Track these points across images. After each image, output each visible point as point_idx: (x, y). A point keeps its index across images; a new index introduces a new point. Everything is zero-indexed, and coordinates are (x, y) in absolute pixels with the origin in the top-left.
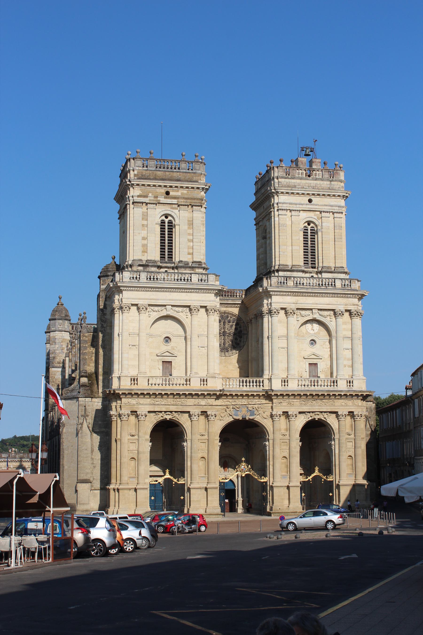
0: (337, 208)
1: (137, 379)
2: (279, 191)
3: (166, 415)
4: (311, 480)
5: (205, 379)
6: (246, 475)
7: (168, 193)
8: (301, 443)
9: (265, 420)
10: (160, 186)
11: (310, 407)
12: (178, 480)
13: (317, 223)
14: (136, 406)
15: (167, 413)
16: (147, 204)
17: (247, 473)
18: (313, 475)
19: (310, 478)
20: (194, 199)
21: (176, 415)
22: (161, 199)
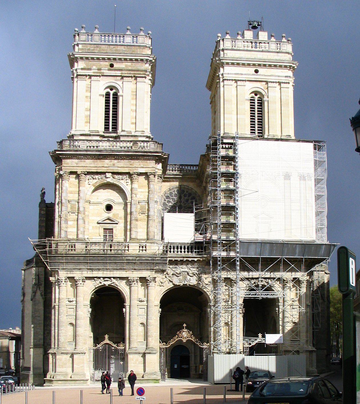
0: (284, 78)
2: (224, 61)
3: (105, 281)
7: (112, 66)
10: (104, 59)
12: (118, 346)
13: (264, 93)
15: (106, 279)
16: (90, 76)
17: (188, 339)
20: (138, 71)
21: (114, 281)
22: (104, 71)
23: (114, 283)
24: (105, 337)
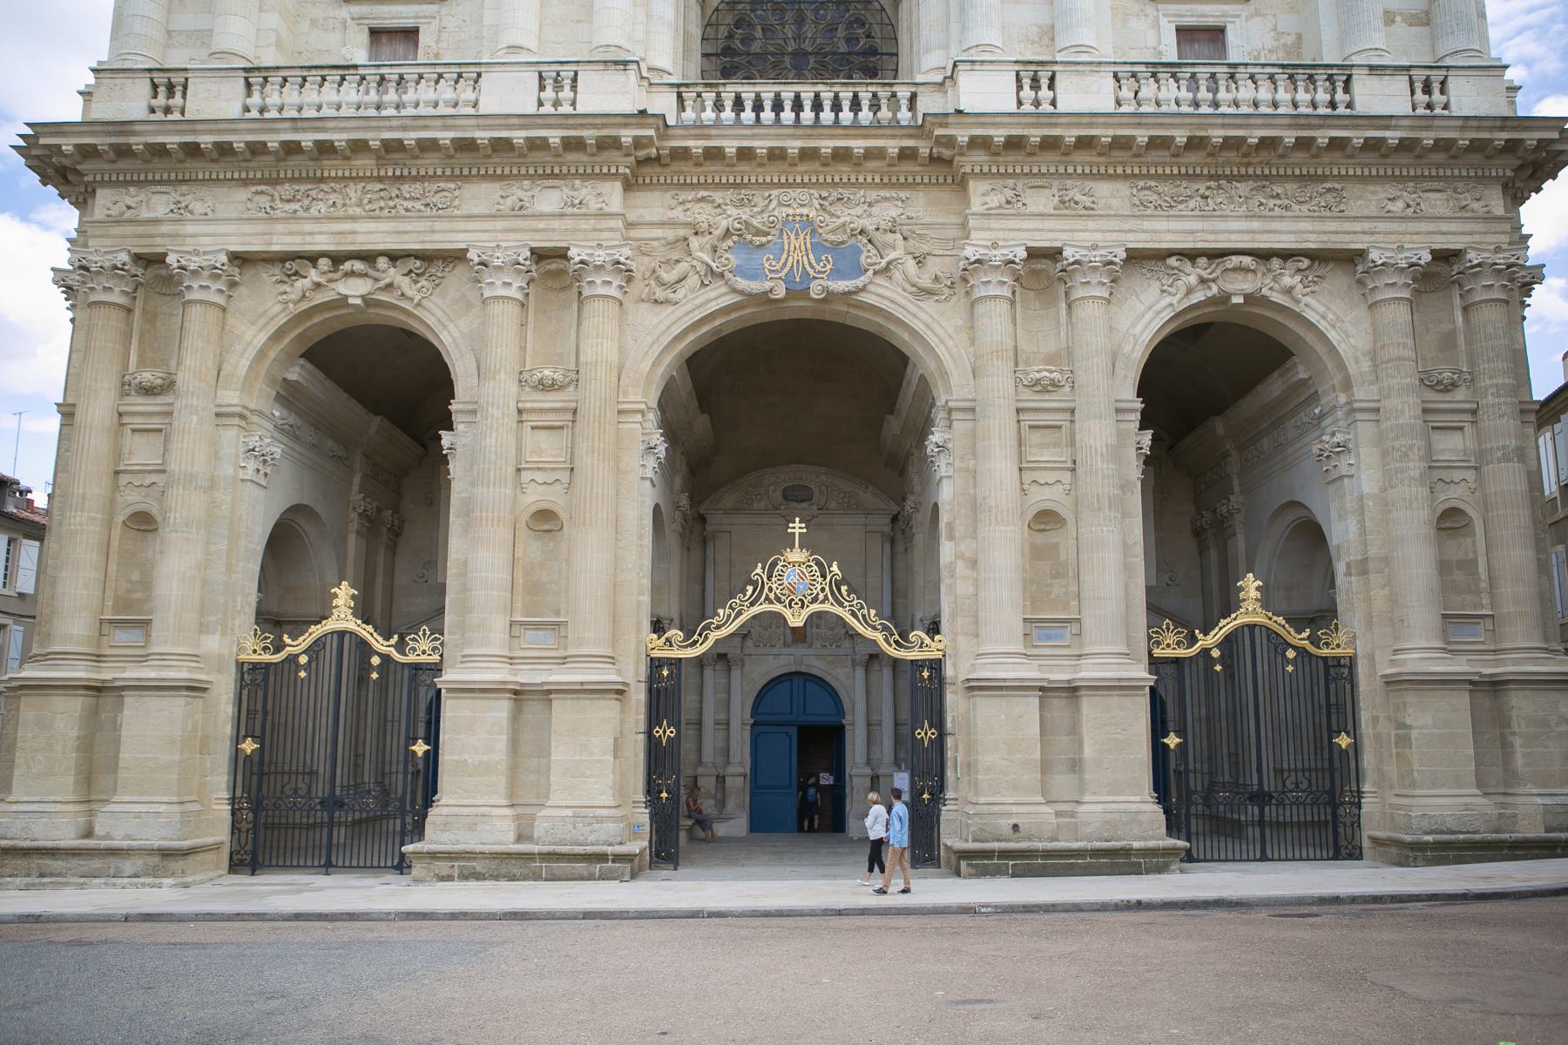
1: (185, 87)
4: (1216, 653)
5: (567, 74)
6: (814, 617)
8: (1147, 438)
9: (929, 305)
11: (1197, 225)
12: (401, 646)
14: (164, 229)
15: (347, 266)
17: (816, 607)
18: (1226, 626)
19: (1209, 640)
21: (393, 274)
23: (390, 286)
24: (336, 596)
